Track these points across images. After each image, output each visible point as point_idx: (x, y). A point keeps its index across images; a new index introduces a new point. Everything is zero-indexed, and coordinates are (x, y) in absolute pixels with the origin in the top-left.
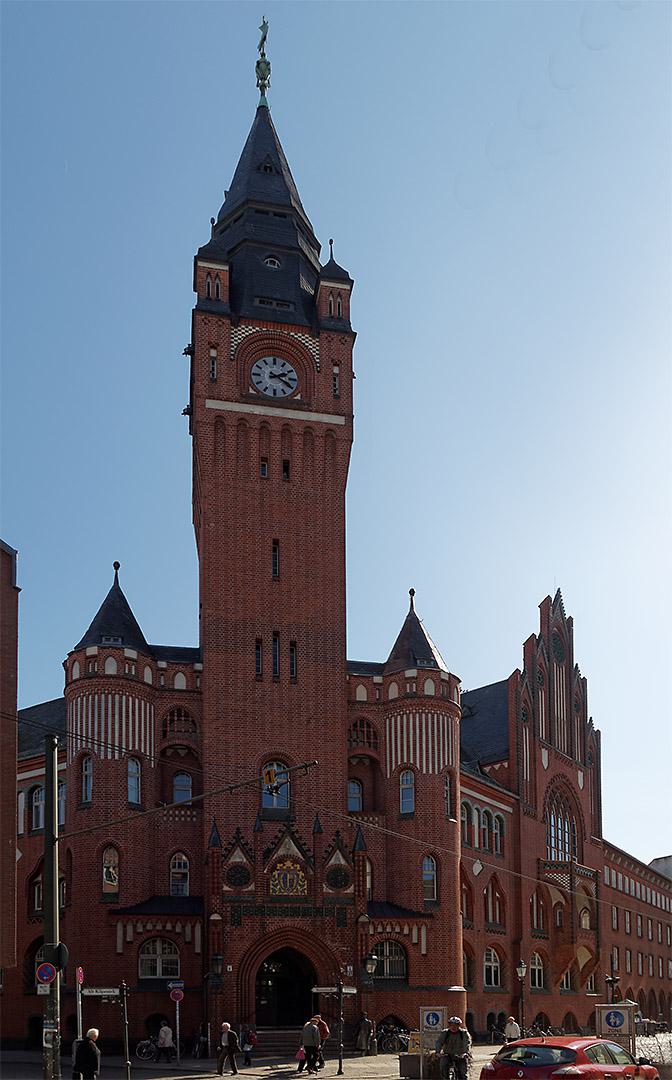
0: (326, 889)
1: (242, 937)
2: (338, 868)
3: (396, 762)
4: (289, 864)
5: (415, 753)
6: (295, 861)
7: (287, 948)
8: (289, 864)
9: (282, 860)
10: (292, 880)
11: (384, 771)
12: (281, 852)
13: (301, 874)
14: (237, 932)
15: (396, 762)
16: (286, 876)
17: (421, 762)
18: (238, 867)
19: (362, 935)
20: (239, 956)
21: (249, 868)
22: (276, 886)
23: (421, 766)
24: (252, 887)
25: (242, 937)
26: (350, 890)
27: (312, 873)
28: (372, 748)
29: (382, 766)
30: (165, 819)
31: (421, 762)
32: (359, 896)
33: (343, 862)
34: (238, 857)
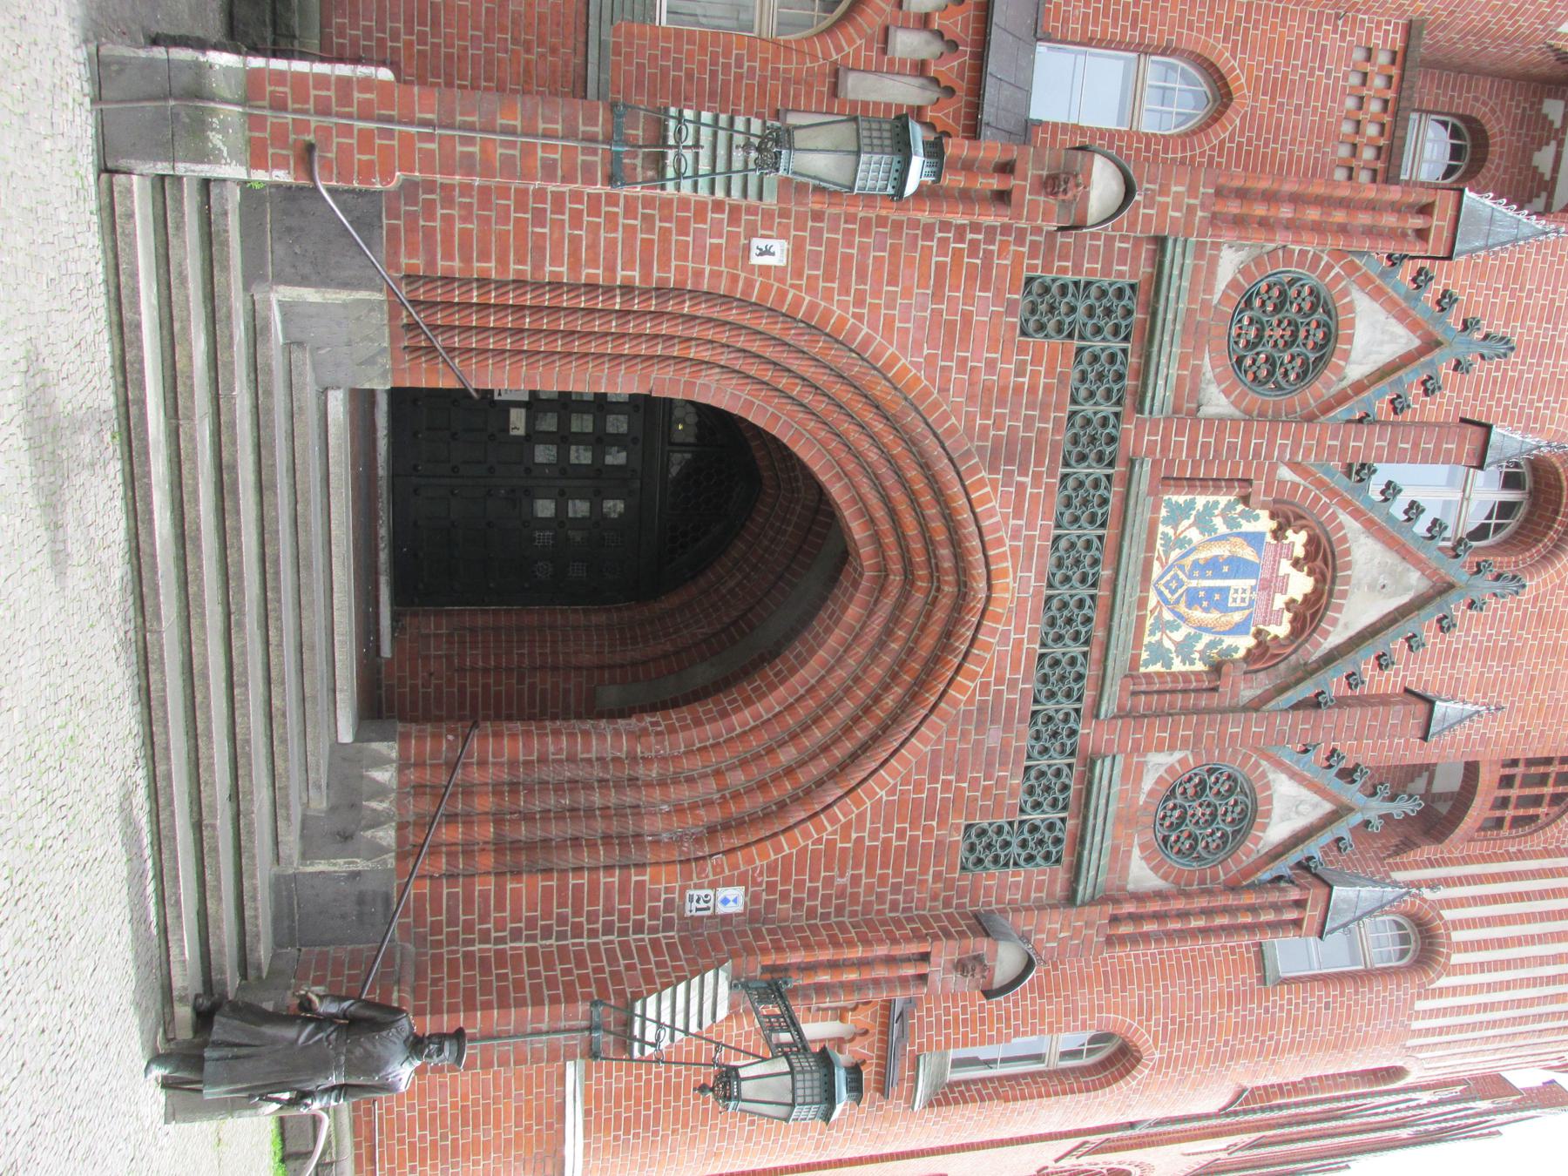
0: (1159, 764)
1: (953, 333)
2: (1248, 817)
3: (1450, 904)
4: (1301, 584)
5: (1482, 967)
6: (1309, 615)
7: (844, 555)
8: (1301, 584)
9: (1323, 558)
10: (1217, 600)
11: (1411, 856)
12: (1365, 554)
13: (1246, 642)
14: (989, 308)
15: (1450, 904)
16: (1238, 567)
17: (1454, 991)
18: (1324, 334)
19: (925, 957)
20: (838, 309)
21: (1325, 386)
22: (1203, 522)
23: (1441, 992)
24: (1217, 402)
25: (953, 333)
26: (1141, 874)
27: (1247, 694)
28: (1488, 814)
29: (1428, 851)
30: (1358, 55)
31: (1454, 991)
32: (1115, 920)
33: (1276, 831)
34: (1373, 337)
